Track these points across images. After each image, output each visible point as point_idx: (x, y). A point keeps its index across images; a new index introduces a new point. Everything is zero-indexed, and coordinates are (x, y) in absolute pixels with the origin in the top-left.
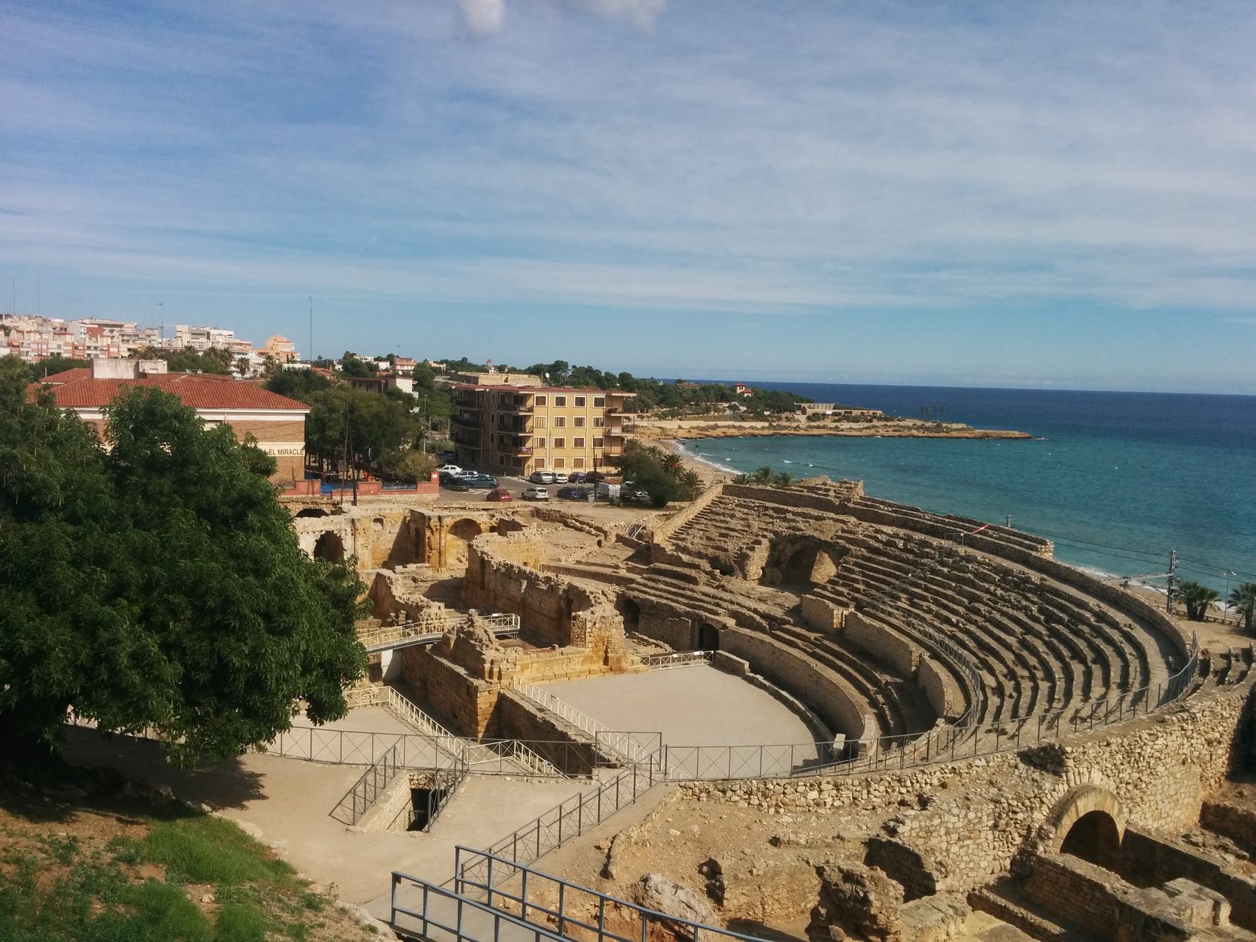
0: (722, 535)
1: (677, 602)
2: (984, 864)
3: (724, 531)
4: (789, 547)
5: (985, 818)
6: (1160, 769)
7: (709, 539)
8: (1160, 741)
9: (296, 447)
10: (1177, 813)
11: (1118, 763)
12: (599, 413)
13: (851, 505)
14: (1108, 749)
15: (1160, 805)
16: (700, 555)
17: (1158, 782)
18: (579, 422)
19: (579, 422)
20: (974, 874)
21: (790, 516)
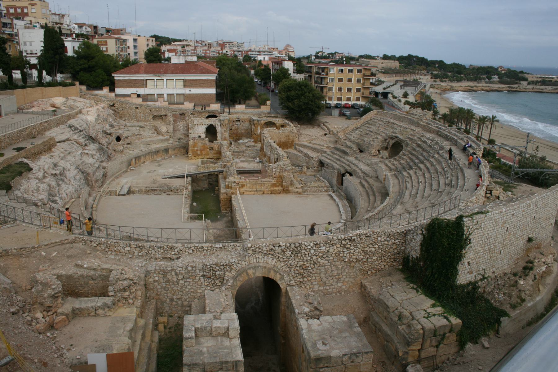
0: (367, 134)
1: (336, 163)
2: (199, 291)
3: (367, 132)
4: (391, 141)
5: (198, 271)
6: (322, 262)
7: (361, 135)
8: (323, 248)
9: (212, 91)
10: (339, 285)
11: (288, 255)
12: (359, 76)
13: (421, 123)
14: (280, 248)
15: (324, 279)
16: (353, 142)
17: (322, 268)
18: (350, 80)
19: (350, 80)
20: (195, 295)
21: (396, 127)
